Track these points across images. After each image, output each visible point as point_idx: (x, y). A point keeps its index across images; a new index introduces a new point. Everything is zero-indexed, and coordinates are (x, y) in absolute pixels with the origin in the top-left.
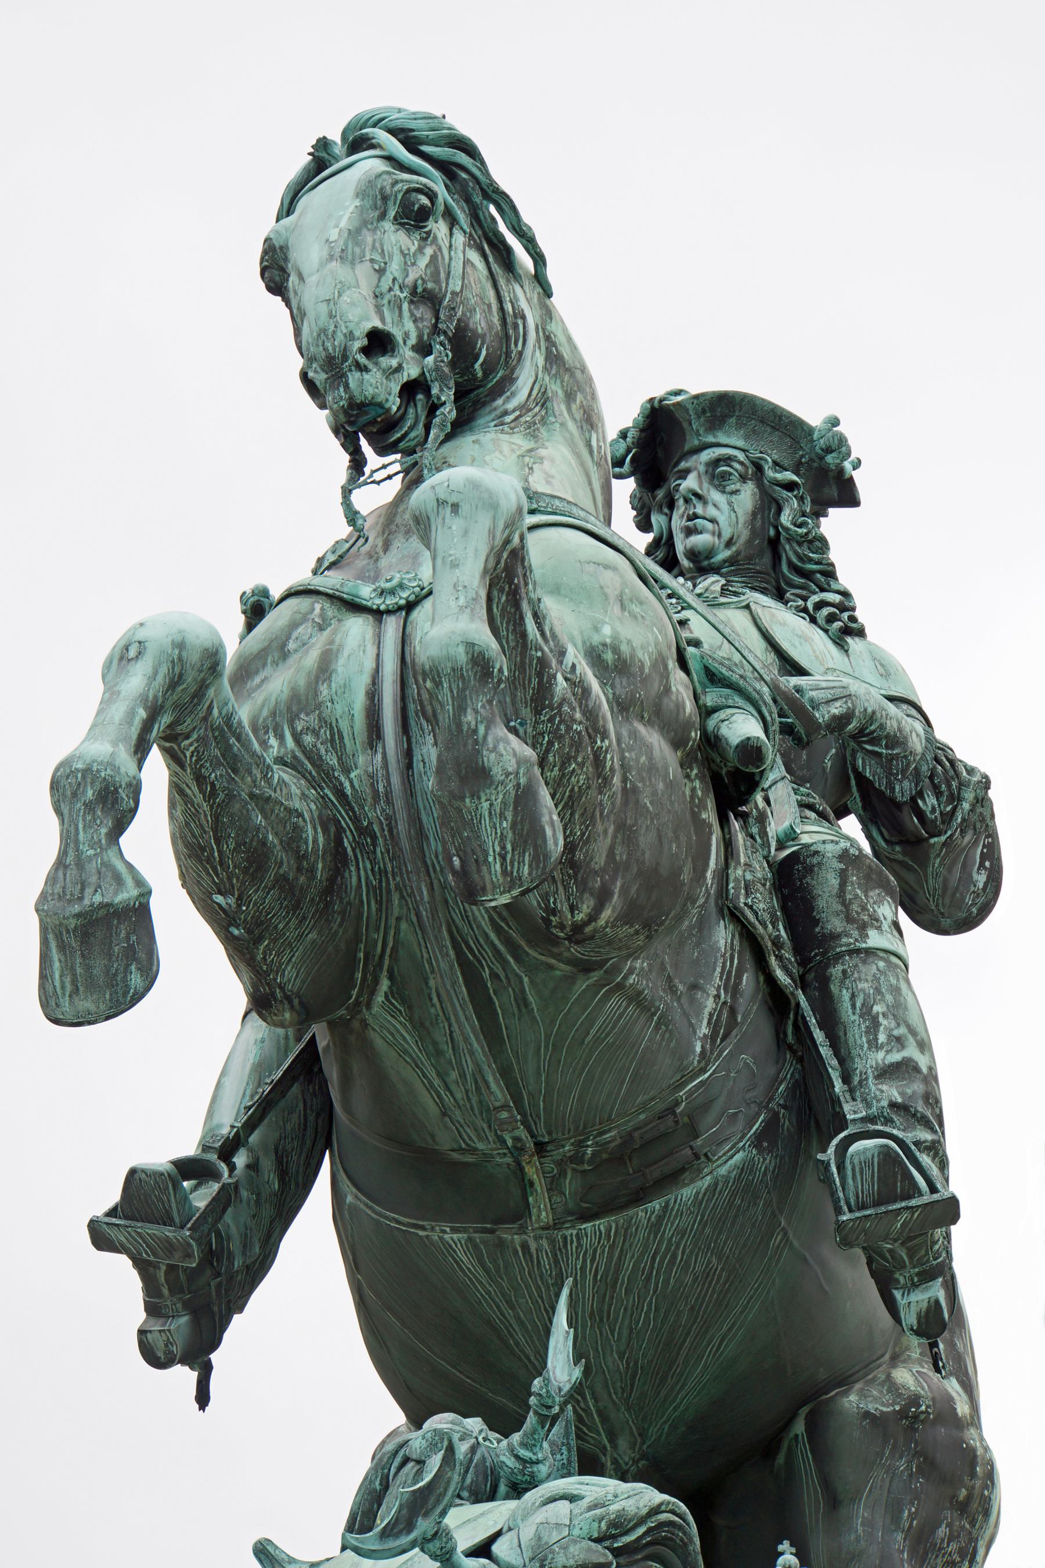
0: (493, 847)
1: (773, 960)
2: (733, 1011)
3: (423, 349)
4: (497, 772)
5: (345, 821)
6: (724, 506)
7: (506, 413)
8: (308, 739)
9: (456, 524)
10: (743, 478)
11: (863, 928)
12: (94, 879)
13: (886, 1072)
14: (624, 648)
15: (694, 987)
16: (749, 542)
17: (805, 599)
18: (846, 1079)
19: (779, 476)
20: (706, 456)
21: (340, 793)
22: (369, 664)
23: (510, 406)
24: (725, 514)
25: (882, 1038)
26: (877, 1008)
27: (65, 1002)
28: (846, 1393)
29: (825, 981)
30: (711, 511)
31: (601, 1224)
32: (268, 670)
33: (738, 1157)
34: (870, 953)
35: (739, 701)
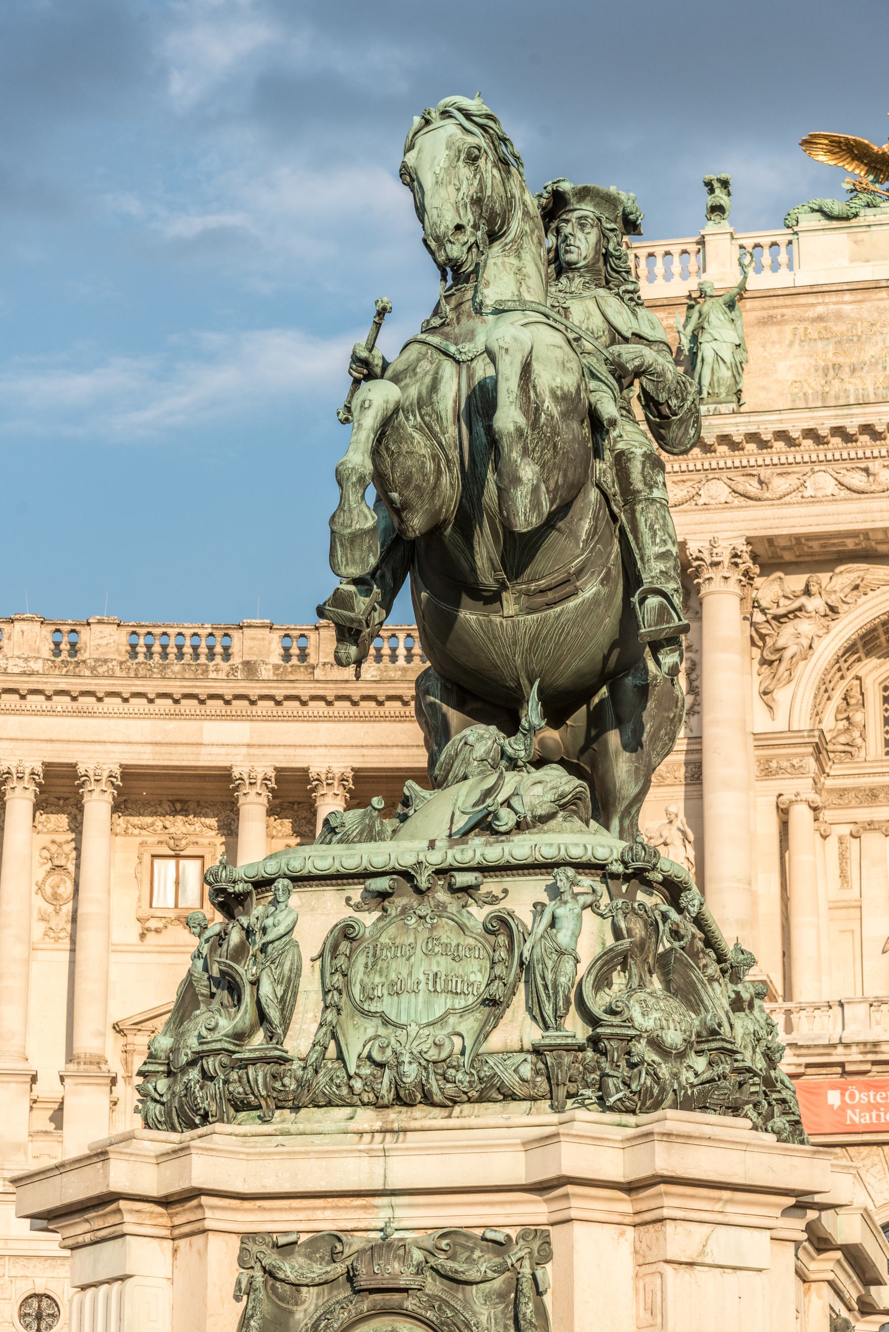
0: (521, 510)
1: (613, 503)
2: (596, 528)
3: (476, 227)
4: (525, 479)
5: (442, 456)
6: (584, 241)
7: (506, 244)
8: (427, 418)
9: (507, 358)
10: (592, 226)
12: (356, 518)
14: (566, 388)
15: (581, 519)
17: (618, 286)
18: (642, 559)
19: (609, 226)
21: (440, 444)
22: (455, 387)
23: (508, 240)
24: (583, 246)
25: (658, 540)
26: (656, 527)
27: (343, 568)
28: (627, 675)
29: (633, 512)
30: (578, 243)
32: (408, 380)
33: (594, 589)
34: (653, 501)
35: (604, 387)
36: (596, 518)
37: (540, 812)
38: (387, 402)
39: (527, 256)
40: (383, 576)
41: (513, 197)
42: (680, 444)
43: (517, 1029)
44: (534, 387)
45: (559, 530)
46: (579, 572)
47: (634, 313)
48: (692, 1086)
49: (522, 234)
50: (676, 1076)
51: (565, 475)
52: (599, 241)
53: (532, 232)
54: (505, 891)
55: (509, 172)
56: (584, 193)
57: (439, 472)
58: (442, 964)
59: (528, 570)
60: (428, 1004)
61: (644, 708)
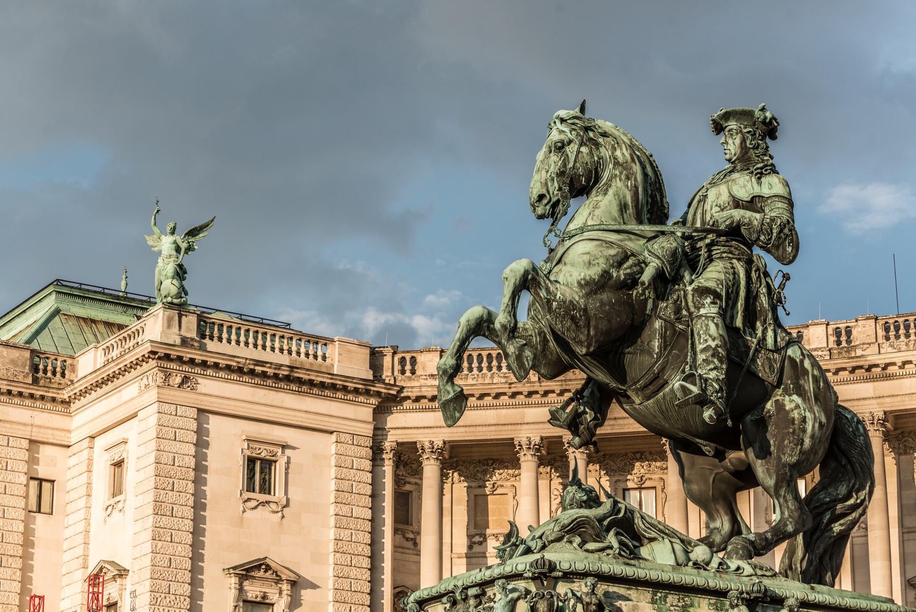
3: (560, 189)
9: (507, 283)
11: (698, 309)
13: (704, 350)
14: (588, 278)
16: (741, 152)
20: (727, 129)
24: (733, 146)
30: (729, 147)
31: (651, 401)
34: (701, 316)
36: (663, 337)
37: (550, 538)
38: (468, 321)
39: (611, 192)
40: (592, 393)
42: (785, 258)
44: (548, 290)
45: (629, 353)
46: (663, 369)
49: (612, 177)
51: (596, 328)
52: (743, 141)
53: (621, 173)
55: (598, 145)
56: (727, 116)
57: (545, 341)
59: (628, 379)
61: (767, 431)
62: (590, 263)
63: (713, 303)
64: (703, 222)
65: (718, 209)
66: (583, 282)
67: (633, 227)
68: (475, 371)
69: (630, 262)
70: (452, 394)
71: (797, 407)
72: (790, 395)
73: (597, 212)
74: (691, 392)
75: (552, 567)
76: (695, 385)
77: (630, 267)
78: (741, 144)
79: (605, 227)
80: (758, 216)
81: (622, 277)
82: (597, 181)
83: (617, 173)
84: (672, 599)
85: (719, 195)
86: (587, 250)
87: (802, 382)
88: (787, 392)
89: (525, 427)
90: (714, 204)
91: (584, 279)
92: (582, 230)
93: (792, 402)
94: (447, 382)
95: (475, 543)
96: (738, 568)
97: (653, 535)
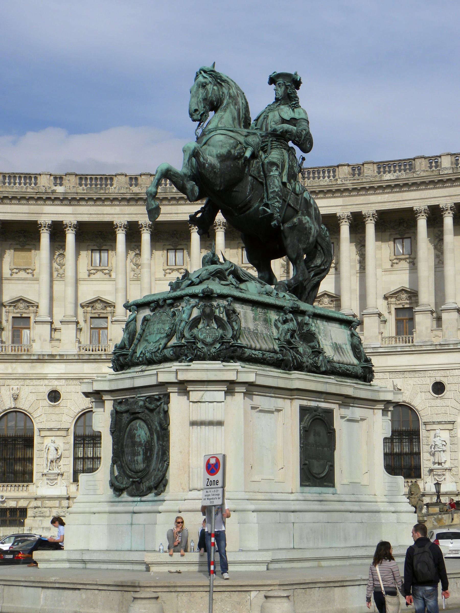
1: (259, 179)
3: (204, 107)
10: (283, 85)
11: (270, 172)
13: (272, 192)
14: (221, 153)
20: (278, 82)
31: (243, 215)
34: (271, 175)
36: (252, 184)
39: (228, 111)
41: (223, 93)
43: (174, 341)
47: (293, 110)
48: (214, 352)
49: (228, 104)
50: (209, 350)
53: (232, 102)
54: (180, 304)
58: (160, 326)
60: (156, 337)
62: (222, 146)
63: (277, 170)
64: (267, 129)
65: (274, 123)
66: (219, 155)
67: (238, 129)
68: (17, 185)
69: (239, 146)
70: (154, 206)
71: (308, 222)
72: (304, 216)
73: (223, 120)
74: (267, 212)
75: (212, 292)
76: (269, 209)
77: (239, 149)
78: (284, 91)
79: (227, 129)
80: (295, 128)
81: (236, 154)
82: (221, 105)
83: (231, 101)
84: (259, 310)
85: (274, 116)
86: (221, 139)
87: (309, 210)
88: (303, 214)
89: (43, 215)
90: (272, 120)
91: (220, 154)
92: (216, 129)
93: (306, 219)
94: (152, 200)
95: (14, 273)
96: (284, 296)
97: (247, 279)
